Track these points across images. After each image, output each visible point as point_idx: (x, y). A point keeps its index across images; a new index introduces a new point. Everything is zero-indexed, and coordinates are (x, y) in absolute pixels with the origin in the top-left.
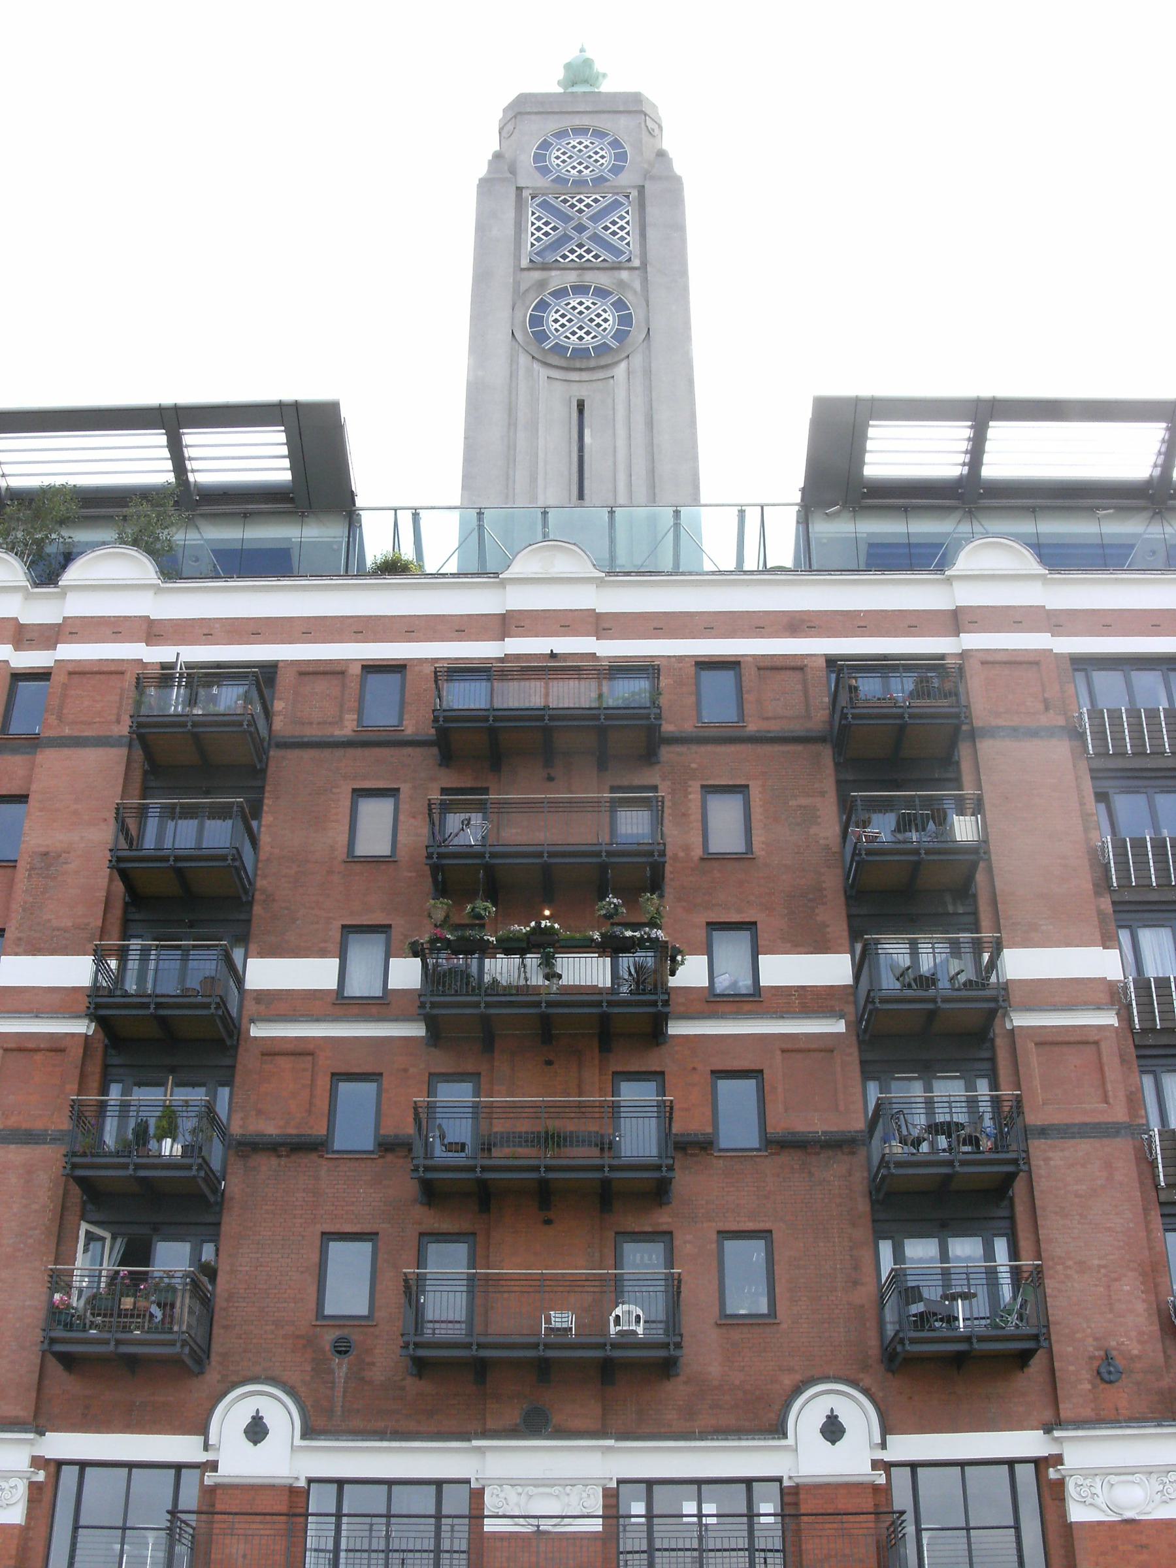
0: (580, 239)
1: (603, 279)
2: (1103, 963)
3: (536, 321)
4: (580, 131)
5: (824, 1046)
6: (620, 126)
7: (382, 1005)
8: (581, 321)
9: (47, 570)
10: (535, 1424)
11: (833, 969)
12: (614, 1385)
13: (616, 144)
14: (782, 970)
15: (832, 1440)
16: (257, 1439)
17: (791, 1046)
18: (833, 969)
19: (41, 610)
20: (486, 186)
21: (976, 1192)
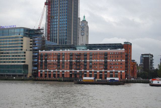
2: (89, 61)
7: (74, 61)
9: (67, 50)
10: (78, 70)
12: (79, 69)
14: (83, 61)
15: (83, 70)
16: (73, 70)
19: (68, 51)
21: (86, 66)
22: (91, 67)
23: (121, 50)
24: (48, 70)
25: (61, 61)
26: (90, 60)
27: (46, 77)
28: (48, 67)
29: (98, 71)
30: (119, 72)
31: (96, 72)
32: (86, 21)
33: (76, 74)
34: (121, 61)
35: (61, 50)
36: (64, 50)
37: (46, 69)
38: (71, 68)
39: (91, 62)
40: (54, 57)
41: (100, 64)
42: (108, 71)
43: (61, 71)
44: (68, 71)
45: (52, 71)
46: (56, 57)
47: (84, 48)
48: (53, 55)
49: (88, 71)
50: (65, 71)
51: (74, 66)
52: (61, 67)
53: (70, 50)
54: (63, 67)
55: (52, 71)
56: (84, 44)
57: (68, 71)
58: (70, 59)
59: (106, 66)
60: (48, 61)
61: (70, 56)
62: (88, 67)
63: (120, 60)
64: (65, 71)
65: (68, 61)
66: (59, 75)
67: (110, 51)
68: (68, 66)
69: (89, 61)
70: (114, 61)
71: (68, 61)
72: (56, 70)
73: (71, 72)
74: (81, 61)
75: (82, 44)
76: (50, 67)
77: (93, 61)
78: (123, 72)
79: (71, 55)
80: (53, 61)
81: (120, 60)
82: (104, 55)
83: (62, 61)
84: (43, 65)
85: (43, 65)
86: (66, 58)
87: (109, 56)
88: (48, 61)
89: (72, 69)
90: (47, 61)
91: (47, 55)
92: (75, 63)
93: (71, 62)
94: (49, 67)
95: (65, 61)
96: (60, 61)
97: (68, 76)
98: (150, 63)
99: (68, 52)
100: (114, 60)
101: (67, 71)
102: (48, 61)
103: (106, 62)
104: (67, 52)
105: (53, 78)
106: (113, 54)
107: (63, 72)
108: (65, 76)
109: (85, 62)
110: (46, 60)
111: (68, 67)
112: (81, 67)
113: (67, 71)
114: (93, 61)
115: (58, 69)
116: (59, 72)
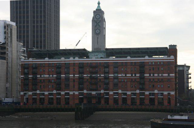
0: (98, 21)
1: (99, 28)
2: (113, 75)
3: (95, 31)
4: (98, 14)
5: (103, 78)
6: (100, 14)
7: (88, 77)
8: (98, 31)
9: (74, 58)
10: (93, 91)
11: (103, 75)
13: (100, 15)
14: (102, 75)
16: (85, 92)
17: (102, 78)
18: (103, 75)
19: (74, 60)
20: (92, 20)
21: (108, 84)
22: (116, 86)
23: (169, 58)
24: (38, 92)
25: (63, 77)
26: (114, 74)
27: (42, 104)
29: (129, 93)
30: (166, 93)
31: (125, 94)
32: (101, 10)
33: (89, 97)
34: (169, 76)
35: (63, 59)
36: (60, 58)
37: (36, 90)
39: (116, 78)
41: (132, 80)
42: (147, 93)
43: (63, 93)
45: (46, 93)
46: (53, 70)
47: (101, 55)
48: (49, 65)
49: (111, 93)
53: (65, 59)
54: (67, 87)
56: (100, 48)
57: (77, 93)
58: (79, 73)
59: (142, 84)
60: (39, 76)
61: (80, 67)
62: (111, 86)
63: (167, 75)
64: (71, 93)
65: (76, 76)
67: (149, 60)
68: (76, 84)
69: (113, 75)
70: (156, 76)
71: (138, 76)
72: (55, 92)
74: (99, 75)
75: (97, 49)
77: (119, 75)
78: (173, 93)
79: (81, 66)
80: (48, 77)
81: (167, 75)
82: (138, 67)
83: (64, 76)
84: (30, 84)
85: (30, 84)
87: (147, 67)
88: (39, 76)
89: (82, 89)
90: (37, 77)
92: (88, 80)
93: (81, 78)
95: (70, 76)
96: (62, 76)
97: (77, 101)
98: (185, 80)
100: (157, 75)
101: (74, 93)
102: (38, 76)
103: (142, 78)
104: (73, 61)
106: (154, 65)
108: (71, 103)
109: (106, 78)
110: (35, 74)
111: (77, 87)
112: (99, 86)
114: (119, 75)
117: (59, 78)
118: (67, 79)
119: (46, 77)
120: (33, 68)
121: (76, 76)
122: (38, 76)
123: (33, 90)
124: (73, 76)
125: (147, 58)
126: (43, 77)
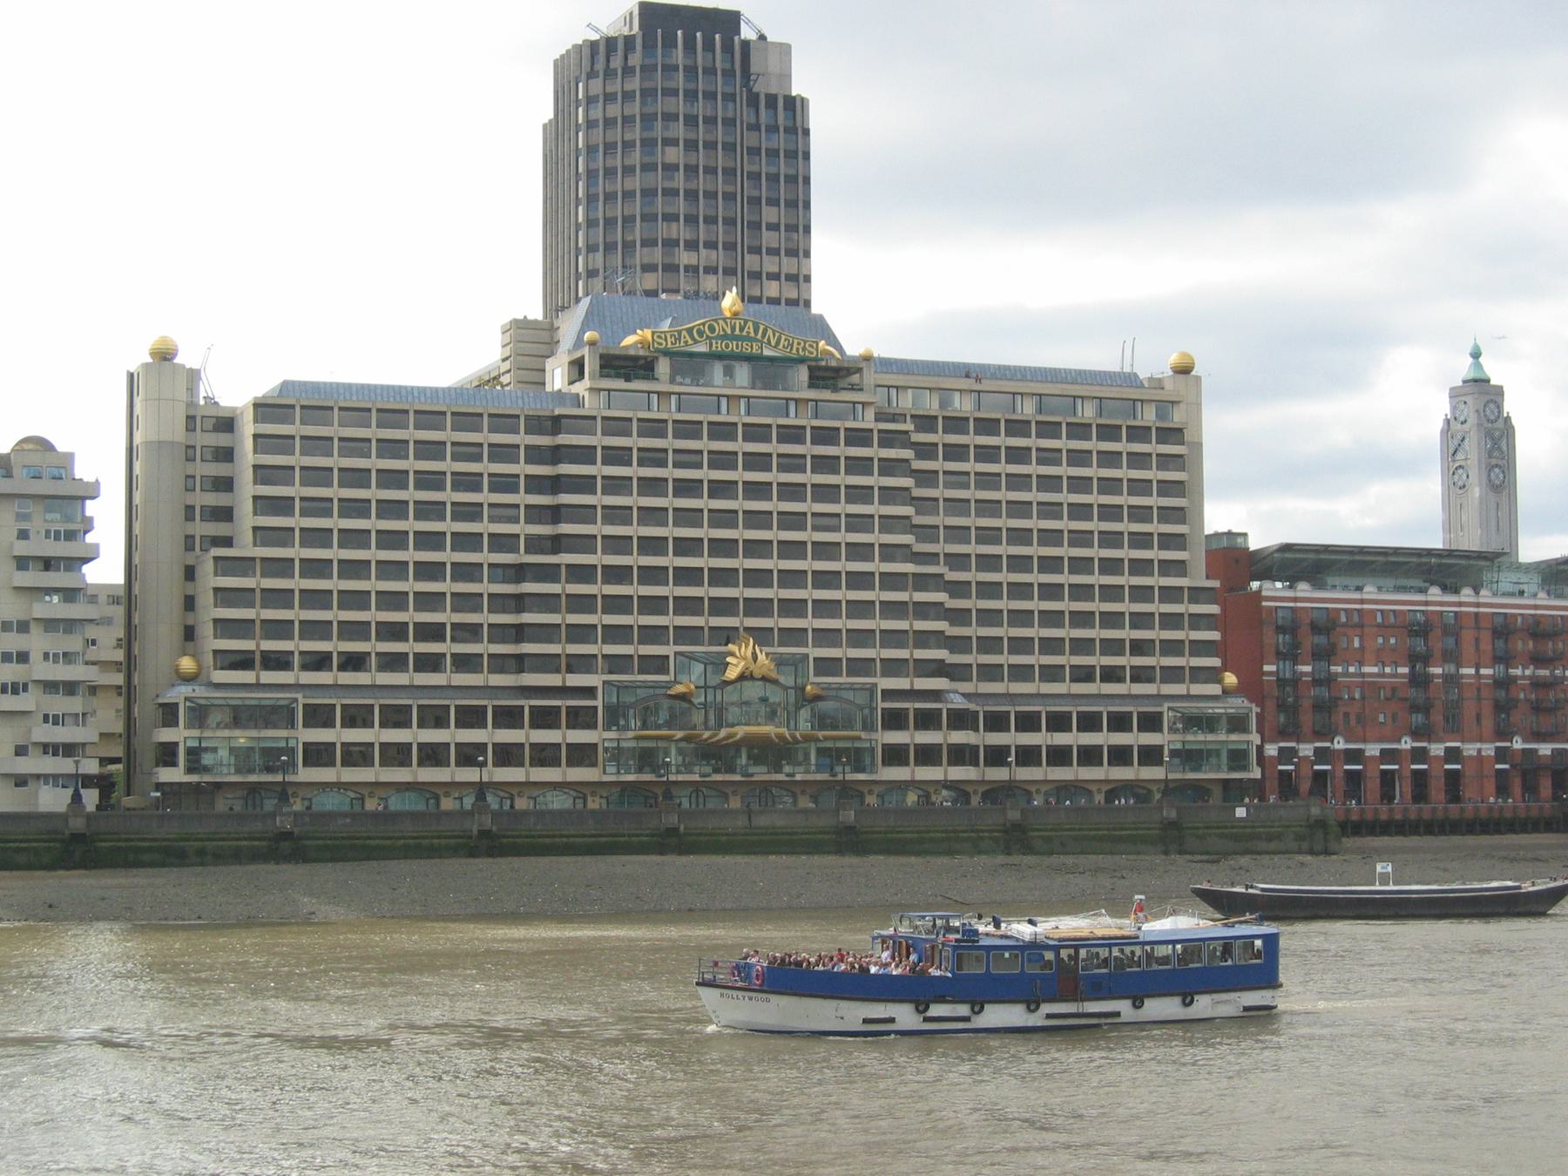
7: (1523, 677)
10: (1544, 741)
16: (1518, 744)
24: (1339, 744)
25: (1438, 676)
28: (1338, 718)
33: (1529, 769)
38: (1503, 733)
40: (1356, 644)
43: (1437, 749)
44: (1488, 749)
45: (1373, 750)
46: (1393, 641)
50: (1470, 749)
51: (1519, 717)
52: (1437, 718)
55: (1373, 750)
57: (1488, 749)
58: (1497, 660)
60: (1339, 669)
64: (1470, 749)
65: (1483, 671)
66: (1420, 779)
72: (1407, 744)
73: (1501, 755)
76: (1353, 717)
80: (1378, 675)
86: (1468, 649)
88: (1339, 669)
91: (1326, 624)
93: (1504, 683)
94: (1346, 715)
97: (1490, 786)
99: (1478, 605)
101: (1479, 751)
105: (1371, 805)
107: (1453, 755)
108: (1469, 791)
111: (1488, 724)
113: (1479, 751)
115: (1416, 734)
116: (1420, 755)
117: (1419, 680)
118: (1451, 680)
119: (1371, 675)
120: (1315, 628)
121: (1483, 671)
122: (1333, 669)
123: (1319, 735)
124: (1472, 671)
125: (1435, 593)
126: (1353, 675)
